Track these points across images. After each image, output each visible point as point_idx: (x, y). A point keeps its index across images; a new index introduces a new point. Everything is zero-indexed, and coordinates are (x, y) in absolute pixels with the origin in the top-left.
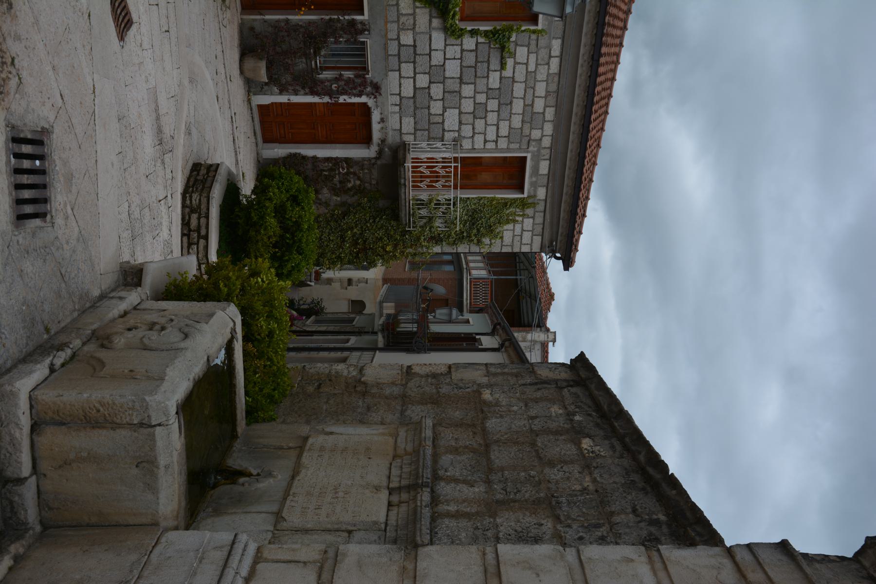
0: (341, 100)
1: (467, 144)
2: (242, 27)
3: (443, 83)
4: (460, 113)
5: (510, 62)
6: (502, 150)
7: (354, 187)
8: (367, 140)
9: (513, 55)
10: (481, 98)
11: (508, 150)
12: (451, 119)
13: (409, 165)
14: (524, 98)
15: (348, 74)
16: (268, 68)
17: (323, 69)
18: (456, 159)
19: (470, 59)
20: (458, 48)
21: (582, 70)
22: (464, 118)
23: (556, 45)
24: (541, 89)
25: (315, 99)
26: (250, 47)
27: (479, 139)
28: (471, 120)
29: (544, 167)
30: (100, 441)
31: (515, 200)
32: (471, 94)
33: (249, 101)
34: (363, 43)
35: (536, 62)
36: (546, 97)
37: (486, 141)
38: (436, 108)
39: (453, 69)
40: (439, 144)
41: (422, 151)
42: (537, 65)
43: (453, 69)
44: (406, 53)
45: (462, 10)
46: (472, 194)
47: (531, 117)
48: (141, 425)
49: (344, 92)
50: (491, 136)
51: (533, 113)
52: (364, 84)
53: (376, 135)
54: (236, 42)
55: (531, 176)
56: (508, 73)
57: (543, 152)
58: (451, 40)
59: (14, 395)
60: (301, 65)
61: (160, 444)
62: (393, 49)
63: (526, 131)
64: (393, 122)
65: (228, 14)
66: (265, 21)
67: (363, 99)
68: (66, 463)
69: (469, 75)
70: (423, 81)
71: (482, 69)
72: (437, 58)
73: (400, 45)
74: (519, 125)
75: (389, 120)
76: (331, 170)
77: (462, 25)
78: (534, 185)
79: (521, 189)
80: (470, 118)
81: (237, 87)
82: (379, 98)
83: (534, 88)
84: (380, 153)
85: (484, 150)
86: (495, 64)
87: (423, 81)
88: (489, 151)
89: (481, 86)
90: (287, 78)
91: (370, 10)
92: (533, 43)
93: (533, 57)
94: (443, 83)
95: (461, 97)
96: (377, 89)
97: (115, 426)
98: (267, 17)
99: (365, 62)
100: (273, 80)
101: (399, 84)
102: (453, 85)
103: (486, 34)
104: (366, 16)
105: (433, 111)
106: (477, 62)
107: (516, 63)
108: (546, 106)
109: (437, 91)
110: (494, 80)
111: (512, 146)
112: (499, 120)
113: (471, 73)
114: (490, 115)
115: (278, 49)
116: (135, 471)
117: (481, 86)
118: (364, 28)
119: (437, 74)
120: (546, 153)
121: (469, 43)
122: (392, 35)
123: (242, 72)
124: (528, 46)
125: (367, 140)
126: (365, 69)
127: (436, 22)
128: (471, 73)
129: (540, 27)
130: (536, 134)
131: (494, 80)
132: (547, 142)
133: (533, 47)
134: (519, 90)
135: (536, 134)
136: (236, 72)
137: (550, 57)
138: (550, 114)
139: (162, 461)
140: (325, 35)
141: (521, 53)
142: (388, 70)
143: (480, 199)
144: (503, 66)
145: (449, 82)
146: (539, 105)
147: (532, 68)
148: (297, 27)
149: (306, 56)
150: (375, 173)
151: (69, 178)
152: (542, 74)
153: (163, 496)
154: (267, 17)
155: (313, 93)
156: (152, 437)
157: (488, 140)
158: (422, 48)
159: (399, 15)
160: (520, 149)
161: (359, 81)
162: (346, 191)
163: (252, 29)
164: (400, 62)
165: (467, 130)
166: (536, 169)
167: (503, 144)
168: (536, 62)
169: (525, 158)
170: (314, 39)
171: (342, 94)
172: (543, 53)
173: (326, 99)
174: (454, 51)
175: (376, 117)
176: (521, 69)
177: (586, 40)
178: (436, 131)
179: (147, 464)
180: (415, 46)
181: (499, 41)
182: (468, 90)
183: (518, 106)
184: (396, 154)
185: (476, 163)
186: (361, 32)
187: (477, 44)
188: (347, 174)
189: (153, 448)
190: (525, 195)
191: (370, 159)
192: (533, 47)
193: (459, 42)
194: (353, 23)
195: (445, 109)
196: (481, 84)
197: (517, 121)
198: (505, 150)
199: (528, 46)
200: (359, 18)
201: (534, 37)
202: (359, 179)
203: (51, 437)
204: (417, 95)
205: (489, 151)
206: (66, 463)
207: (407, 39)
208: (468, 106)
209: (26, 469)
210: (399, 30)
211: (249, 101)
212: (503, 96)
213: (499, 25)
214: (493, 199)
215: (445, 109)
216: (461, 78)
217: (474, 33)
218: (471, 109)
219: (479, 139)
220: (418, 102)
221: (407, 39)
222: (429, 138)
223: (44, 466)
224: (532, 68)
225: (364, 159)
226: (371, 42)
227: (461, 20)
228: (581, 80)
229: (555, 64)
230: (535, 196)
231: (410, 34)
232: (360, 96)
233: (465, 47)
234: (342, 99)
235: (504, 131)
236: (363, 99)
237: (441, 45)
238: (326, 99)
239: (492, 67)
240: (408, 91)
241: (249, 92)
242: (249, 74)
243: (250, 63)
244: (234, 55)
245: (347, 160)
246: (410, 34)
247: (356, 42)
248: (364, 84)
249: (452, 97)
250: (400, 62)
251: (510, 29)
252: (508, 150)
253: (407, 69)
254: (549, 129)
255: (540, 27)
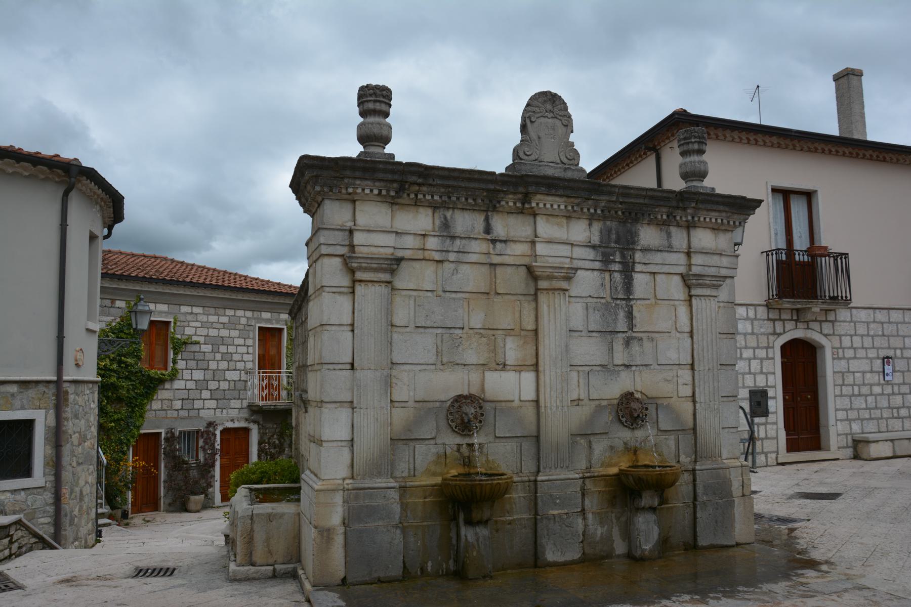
0: (219, 447)
1: (249, 365)
2: (168, 511)
3: (207, 381)
4: (228, 370)
5: (195, 338)
6: (254, 343)
7: (278, 440)
8: (246, 431)
9: (190, 336)
10: (218, 356)
11: (254, 339)
12: (232, 375)
13: (261, 403)
14: (219, 329)
15: (201, 443)
16: (195, 494)
17: (197, 459)
18: (259, 373)
19: (192, 364)
20: (185, 372)
21: (201, 292)
22: (231, 367)
23: (184, 309)
24: (213, 319)
25: (218, 464)
26: (181, 506)
27: (246, 357)
28: (233, 363)
29: (266, 315)
30: (259, 537)
31: (288, 333)
32: (215, 363)
33: (218, 507)
34: (180, 432)
35: (194, 322)
36: (218, 315)
37: (248, 353)
38: (224, 385)
39: (198, 375)
40: (249, 383)
41: (254, 394)
42: (197, 321)
43: (198, 375)
44: (187, 405)
45: (160, 369)
46: (284, 362)
47: (232, 324)
48: (252, 519)
49: (213, 445)
50: (244, 350)
51: (229, 323)
52: (207, 432)
53: (243, 424)
54: (178, 514)
55: (272, 324)
56: (202, 339)
57: (255, 316)
58: (179, 376)
59: (234, 571)
60: (194, 473)
61: (261, 512)
62: (184, 413)
63: (241, 327)
64: (234, 413)
65: (158, 519)
66: (165, 496)
67: (218, 433)
68: (270, 552)
69: (203, 365)
70: (206, 394)
71: (199, 356)
72: (191, 385)
73: (182, 409)
74: (237, 332)
75: (232, 416)
76: (266, 454)
77: (170, 369)
78: (278, 322)
79: (281, 330)
80: (232, 363)
81: (206, 514)
82: (218, 422)
83: (212, 323)
84: (255, 422)
85: (253, 354)
86: (195, 348)
87: (206, 394)
88: (254, 351)
89: (210, 356)
90: (203, 483)
91: (158, 428)
92: (182, 324)
93: (192, 324)
94: (207, 381)
95: (218, 370)
96: (211, 424)
97: (252, 530)
98: (162, 494)
99: (193, 431)
100: (204, 491)
101: (208, 410)
102: (209, 375)
103: (175, 354)
104: (163, 431)
105: (227, 388)
106: (194, 360)
107: (195, 334)
108: (225, 315)
109: (213, 385)
110: (206, 348)
111: (251, 336)
112: (233, 345)
113: (201, 363)
114: (230, 351)
115: (184, 488)
116: (274, 523)
117: (210, 356)
118: (170, 432)
119: (201, 385)
120: (256, 314)
121: (181, 364)
122: (175, 414)
123: (198, 511)
124: (184, 327)
125: (246, 431)
126: (198, 432)
127: (167, 386)
128: (201, 363)
129: (172, 320)
130: (243, 321)
131: (206, 348)
132: (249, 314)
133: (185, 324)
134: (213, 332)
135: (243, 321)
136: (197, 515)
137: (192, 313)
138: (230, 312)
139: (270, 511)
140: (174, 457)
141: (189, 331)
142: (198, 416)
143: (287, 356)
144: (197, 343)
145: (207, 377)
146: (224, 319)
147: (199, 324)
148: (169, 476)
149: (187, 470)
150: (269, 425)
151: (164, 561)
152: (205, 318)
153: (286, 511)
154: (162, 494)
155: (213, 465)
156: (258, 515)
157: (247, 351)
158: (184, 394)
159: (162, 409)
160: (254, 331)
161: (205, 436)
162: (281, 444)
163: (170, 505)
164: (193, 409)
165: (240, 365)
166: (267, 321)
167: (249, 342)
168: (194, 322)
169: (259, 328)
170: (177, 465)
171: (214, 446)
172: (189, 317)
173: (218, 457)
174: (186, 375)
175: (230, 425)
176: (200, 331)
177: (181, 291)
178: (240, 385)
179: (270, 517)
180: (183, 399)
181: (180, 345)
182: (213, 365)
183: (224, 333)
184: (255, 411)
185: (261, 358)
186: (173, 434)
187: (182, 359)
188: (269, 444)
189: (263, 515)
190: (285, 327)
191: (259, 429)
192: (185, 324)
193: (180, 371)
194: (166, 439)
195: (226, 380)
196: (209, 356)
197: (234, 333)
198: (253, 340)
199: (184, 327)
200: (163, 435)
201: (178, 324)
202: (273, 436)
203: (258, 556)
204: (216, 397)
205: (254, 351)
206: (270, 552)
207: (178, 404)
208: (223, 365)
209: (271, 568)
210: (172, 409)
211: (218, 507)
212: (217, 342)
213: (170, 346)
214: (287, 348)
215: (226, 380)
216: (205, 370)
217: (175, 362)
218: (226, 363)
219: (246, 357)
220: (220, 397)
221: (178, 404)
222: (245, 390)
223: (271, 561)
224: (199, 324)
225: (259, 433)
226: (179, 428)
227: (166, 369)
228: (208, 293)
229: (196, 310)
230: (286, 321)
231: (174, 402)
232: (215, 435)
233: (184, 367)
234: (218, 447)
235: (241, 341)
236: (218, 433)
237: (183, 382)
238: (218, 457)
239: (198, 350)
240: (213, 404)
241: (212, 507)
242: (199, 507)
243: (192, 506)
244: (186, 516)
245: (260, 444)
246: (174, 402)
247: (179, 437)
248: (207, 432)
249: (217, 375)
250: (193, 409)
251: (173, 338)
252: (254, 339)
253: (198, 404)
254: (240, 313)
255: (172, 320)
